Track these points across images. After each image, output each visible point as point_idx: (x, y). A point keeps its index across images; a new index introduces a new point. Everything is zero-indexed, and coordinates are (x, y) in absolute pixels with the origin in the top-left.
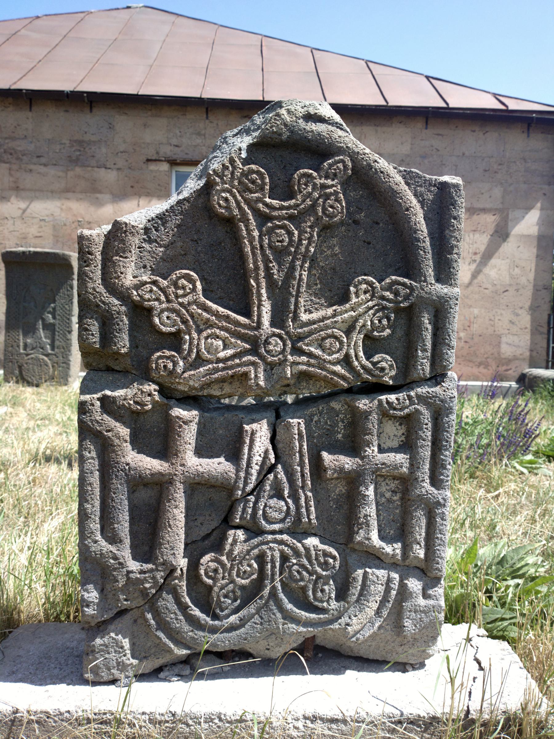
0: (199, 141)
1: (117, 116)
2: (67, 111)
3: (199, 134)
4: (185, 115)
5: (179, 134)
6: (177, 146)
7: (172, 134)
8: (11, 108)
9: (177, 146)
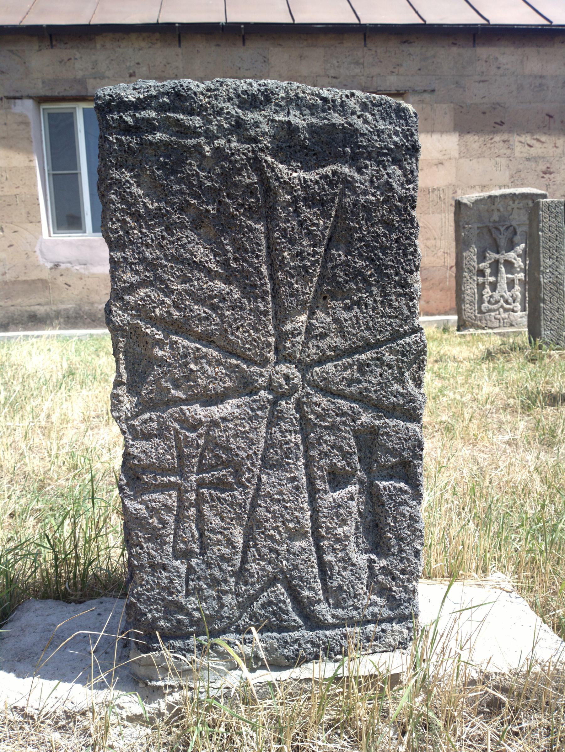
0: (357, 70)
1: (272, 48)
2: (218, 45)
3: (357, 63)
4: (342, 43)
5: (336, 64)
6: (335, 78)
7: (329, 65)
8: (159, 44)
9: (335, 78)
